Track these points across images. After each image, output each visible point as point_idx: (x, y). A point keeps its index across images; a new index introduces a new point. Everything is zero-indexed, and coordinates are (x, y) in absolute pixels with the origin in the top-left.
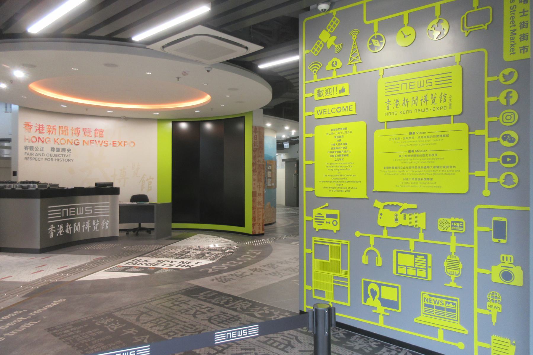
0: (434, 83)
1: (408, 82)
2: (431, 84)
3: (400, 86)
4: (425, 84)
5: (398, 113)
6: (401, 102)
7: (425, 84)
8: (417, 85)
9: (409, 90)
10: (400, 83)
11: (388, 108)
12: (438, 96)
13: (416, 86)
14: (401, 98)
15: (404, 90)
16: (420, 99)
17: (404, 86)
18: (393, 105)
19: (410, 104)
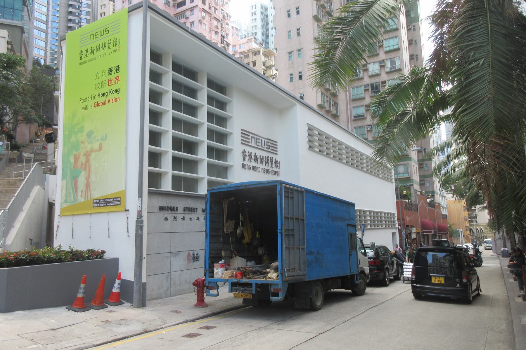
4: (266, 146)
11: (244, 160)
12: (274, 160)
15: (253, 145)
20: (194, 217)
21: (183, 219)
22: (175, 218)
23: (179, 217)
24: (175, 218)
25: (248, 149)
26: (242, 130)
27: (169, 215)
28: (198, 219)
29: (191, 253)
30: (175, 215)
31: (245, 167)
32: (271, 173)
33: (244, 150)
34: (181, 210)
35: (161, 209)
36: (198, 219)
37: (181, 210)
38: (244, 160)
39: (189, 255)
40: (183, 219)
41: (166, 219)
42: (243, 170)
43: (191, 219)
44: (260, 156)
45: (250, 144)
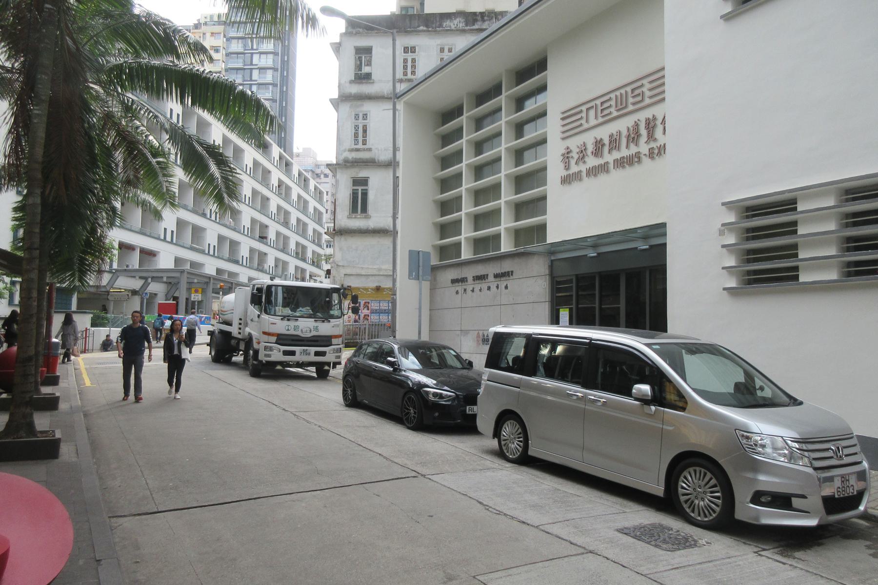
0: (648, 93)
1: (598, 102)
2: (640, 98)
3: (584, 115)
5: (584, 174)
6: (590, 148)
7: (631, 100)
8: (613, 103)
9: (601, 120)
10: (584, 108)
13: (613, 110)
14: (589, 139)
15: (593, 122)
16: (625, 133)
17: (592, 113)
18: (576, 156)
19: (606, 149)
20: (484, 286)
21: (473, 291)
22: (465, 290)
23: (469, 288)
24: (465, 290)
25: (574, 143)
26: (563, 113)
27: (459, 287)
28: (489, 288)
29: (481, 333)
30: (465, 287)
31: (566, 180)
32: (646, 160)
33: (568, 148)
34: (470, 279)
35: (454, 281)
36: (489, 288)
37: (470, 279)
38: (567, 168)
39: (478, 336)
40: (473, 291)
41: (457, 292)
42: (567, 188)
43: (480, 290)
44: (611, 136)
45: (586, 126)
